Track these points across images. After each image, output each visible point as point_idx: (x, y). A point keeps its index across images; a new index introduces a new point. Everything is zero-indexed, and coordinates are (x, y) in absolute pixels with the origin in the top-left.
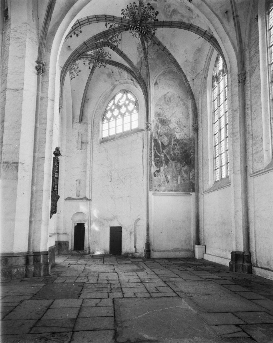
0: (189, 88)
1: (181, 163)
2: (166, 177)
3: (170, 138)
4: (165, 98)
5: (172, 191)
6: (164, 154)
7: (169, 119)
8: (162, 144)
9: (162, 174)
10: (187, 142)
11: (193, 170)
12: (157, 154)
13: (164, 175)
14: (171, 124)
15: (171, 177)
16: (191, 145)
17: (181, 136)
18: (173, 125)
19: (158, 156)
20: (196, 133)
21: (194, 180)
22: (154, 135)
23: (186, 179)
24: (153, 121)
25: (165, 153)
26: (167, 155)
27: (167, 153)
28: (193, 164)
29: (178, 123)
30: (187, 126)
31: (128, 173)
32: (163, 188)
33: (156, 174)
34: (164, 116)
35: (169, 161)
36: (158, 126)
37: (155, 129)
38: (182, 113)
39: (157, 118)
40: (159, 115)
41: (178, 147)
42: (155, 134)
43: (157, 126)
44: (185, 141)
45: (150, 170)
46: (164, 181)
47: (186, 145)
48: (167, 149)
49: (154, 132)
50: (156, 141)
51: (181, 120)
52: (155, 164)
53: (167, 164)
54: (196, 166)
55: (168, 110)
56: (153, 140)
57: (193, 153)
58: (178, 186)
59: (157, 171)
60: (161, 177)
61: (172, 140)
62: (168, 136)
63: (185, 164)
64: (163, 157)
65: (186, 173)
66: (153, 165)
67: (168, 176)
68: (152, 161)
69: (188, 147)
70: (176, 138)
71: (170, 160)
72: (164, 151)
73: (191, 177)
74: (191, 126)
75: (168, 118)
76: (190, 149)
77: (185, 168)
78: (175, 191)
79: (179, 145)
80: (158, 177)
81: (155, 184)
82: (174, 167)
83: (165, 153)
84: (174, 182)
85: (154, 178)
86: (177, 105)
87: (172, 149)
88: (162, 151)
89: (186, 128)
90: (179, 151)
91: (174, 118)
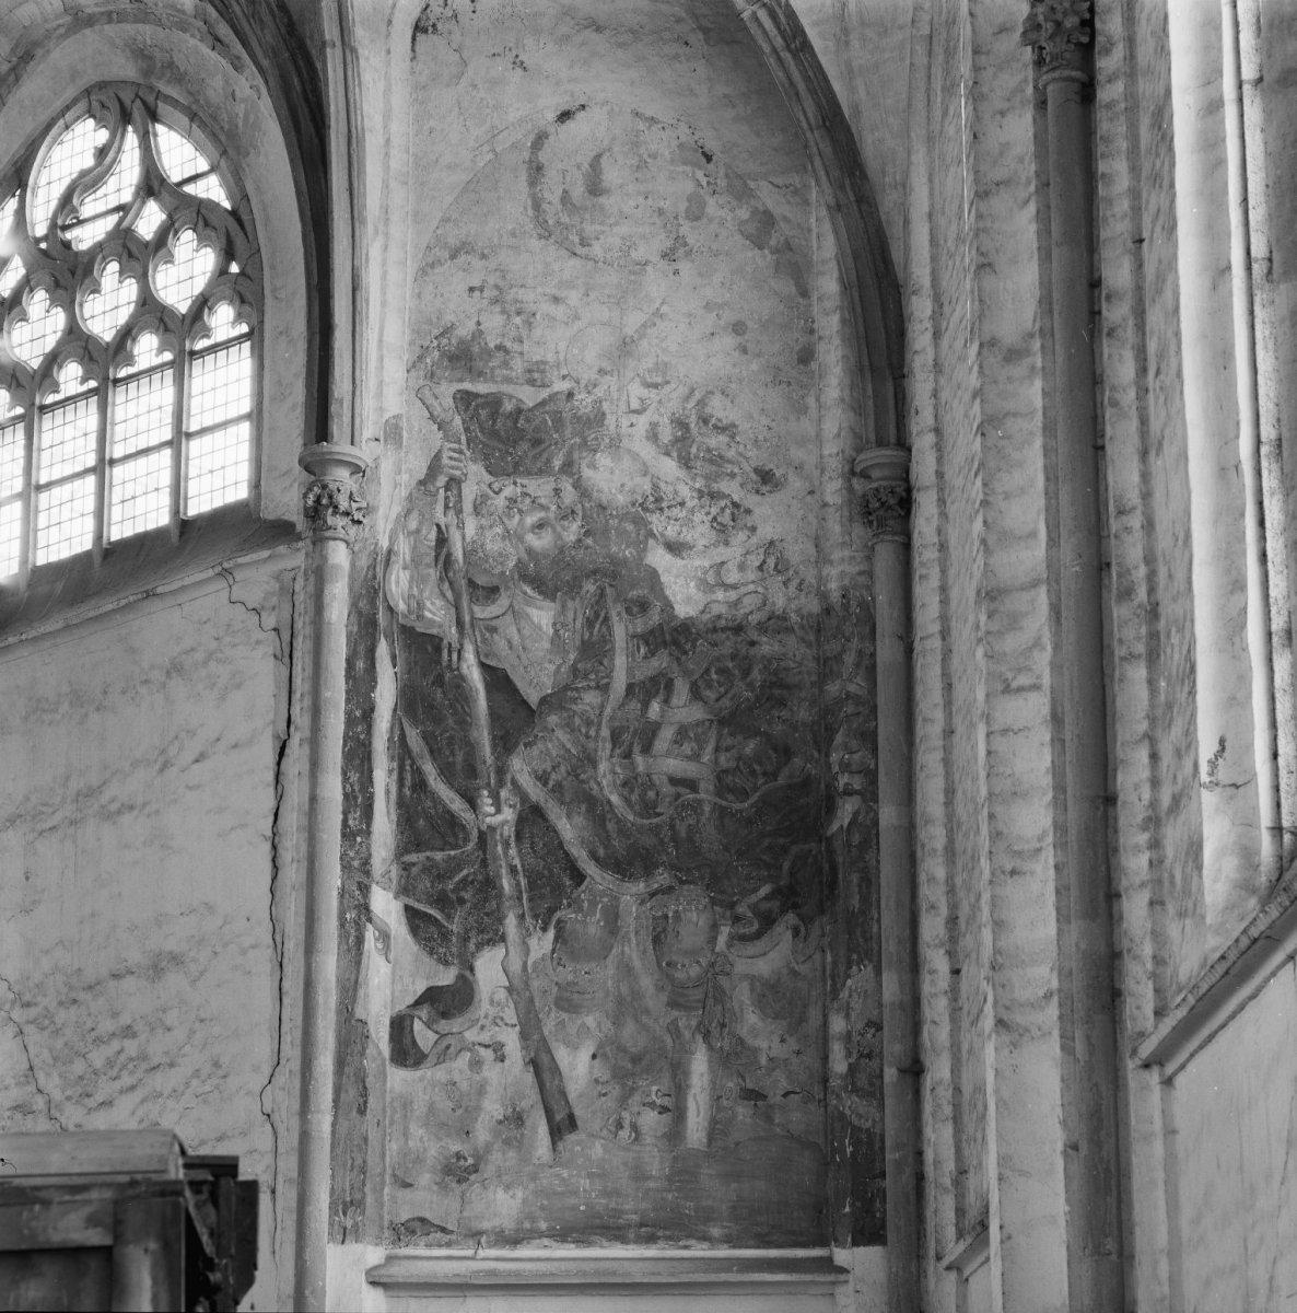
0: (786, 56)
1: (723, 902)
2: (541, 1066)
3: (597, 617)
4: (536, 170)
5: (613, 1230)
6: (524, 797)
7: (584, 402)
8: (498, 680)
9: (485, 1037)
10: (795, 652)
11: (860, 978)
12: (436, 800)
13: (511, 1040)
14: (603, 459)
15: (602, 1072)
16: (833, 688)
17: (727, 587)
18: (627, 462)
20: (885, 556)
21: (875, 1092)
22: (398, 584)
23: (784, 1084)
24: (392, 433)
27: (557, 789)
28: (855, 902)
29: (681, 445)
30: (799, 468)
31: (128, 1032)
32: (502, 1204)
33: (423, 1035)
34: (518, 366)
35: (579, 877)
36: (454, 483)
37: (415, 515)
38: (738, 328)
39: (447, 390)
40: (462, 357)
41: (683, 709)
42: (418, 579)
43: (436, 481)
44: (767, 647)
45: (350, 989)
46: (517, 1119)
47: (776, 690)
48: (555, 740)
49: (404, 548)
50: (423, 650)
51: (718, 408)
52: (413, 917)
53: (552, 911)
54: (889, 922)
55: (574, 297)
56: (383, 649)
57: (857, 783)
58: (683, 1173)
59: (431, 996)
60: (476, 1064)
61: (619, 632)
62: (573, 588)
63: (775, 905)
64: (509, 831)
65: (776, 1017)
66: (385, 937)
67: (562, 1055)
68: (364, 889)
69: (804, 714)
70: (668, 606)
71: (590, 869)
72: (521, 767)
73: (839, 1064)
74: (835, 465)
75: (570, 395)
76: (822, 735)
77: (772, 957)
78: (650, 1239)
79: (696, 694)
80: (440, 1074)
81: (404, 1153)
82: (634, 949)
83: (535, 792)
84: (635, 1128)
85: (398, 1078)
86: (680, 241)
87: (615, 738)
88: (501, 771)
89: (778, 496)
91: (636, 391)
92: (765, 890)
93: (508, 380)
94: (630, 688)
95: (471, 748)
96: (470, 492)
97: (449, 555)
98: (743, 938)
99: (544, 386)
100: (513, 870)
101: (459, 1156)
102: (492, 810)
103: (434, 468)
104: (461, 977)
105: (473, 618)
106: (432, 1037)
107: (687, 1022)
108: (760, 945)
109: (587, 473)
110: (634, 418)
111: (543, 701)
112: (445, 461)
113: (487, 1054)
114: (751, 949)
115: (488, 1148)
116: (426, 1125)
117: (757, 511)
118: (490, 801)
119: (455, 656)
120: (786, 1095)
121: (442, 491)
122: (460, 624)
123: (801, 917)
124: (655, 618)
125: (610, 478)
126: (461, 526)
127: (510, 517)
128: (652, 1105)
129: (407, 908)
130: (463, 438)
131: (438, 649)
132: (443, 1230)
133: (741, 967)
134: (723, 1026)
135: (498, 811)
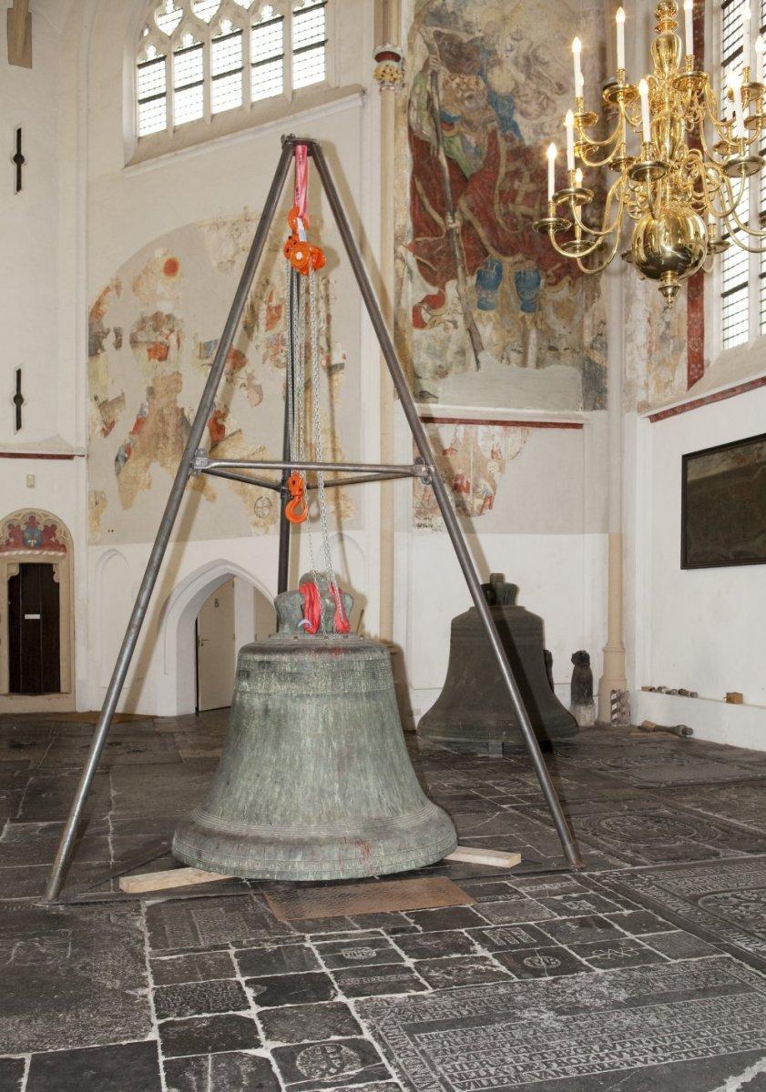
2: (472, 331)
9: (450, 318)
19: (434, 228)
23: (565, 345)
25: (469, 216)
26: (476, 224)
33: (426, 316)
35: (487, 254)
36: (434, 74)
42: (420, 116)
43: (427, 71)
53: (476, 266)
60: (446, 329)
64: (458, 231)
67: (480, 327)
70: (521, 139)
71: (491, 250)
79: (532, 180)
82: (507, 285)
87: (501, 193)
88: (455, 205)
90: (532, 207)
92: (558, 265)
93: (457, 29)
94: (507, 174)
95: (443, 193)
96: (441, 78)
97: (433, 105)
98: (551, 284)
99: (471, 33)
100: (460, 248)
101: (440, 367)
102: (451, 221)
103: (426, 65)
104: (440, 292)
105: (443, 137)
106: (429, 316)
107: (528, 317)
108: (557, 287)
109: (489, 76)
110: (509, 54)
111: (472, 175)
112: (431, 63)
113: (451, 325)
114: (553, 289)
115: (451, 364)
116: (427, 353)
117: (558, 102)
118: (450, 217)
119: (436, 152)
120: (565, 349)
121: (429, 77)
122: (438, 137)
123: (572, 277)
124: (517, 143)
125: (501, 80)
126: (438, 94)
127: (458, 92)
128: (515, 350)
129: (418, 261)
130: (438, 54)
131: (428, 149)
132: (435, 397)
133: (549, 296)
134: (542, 320)
135: (454, 222)
